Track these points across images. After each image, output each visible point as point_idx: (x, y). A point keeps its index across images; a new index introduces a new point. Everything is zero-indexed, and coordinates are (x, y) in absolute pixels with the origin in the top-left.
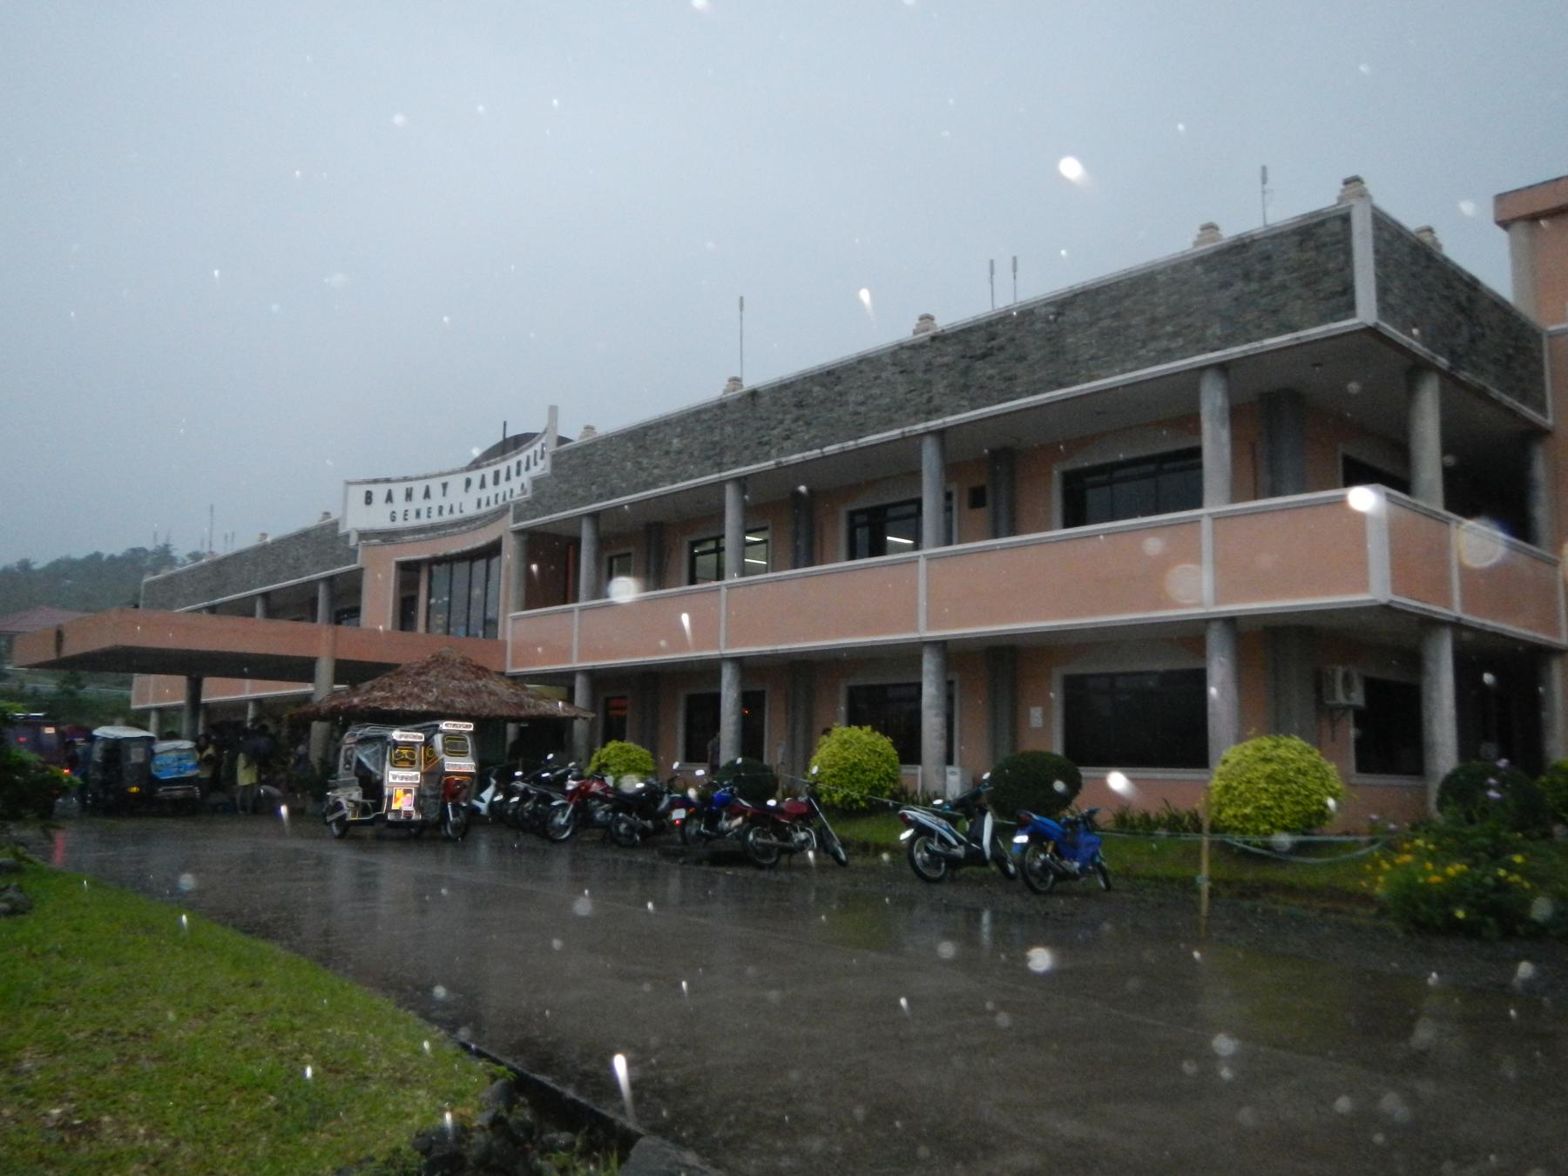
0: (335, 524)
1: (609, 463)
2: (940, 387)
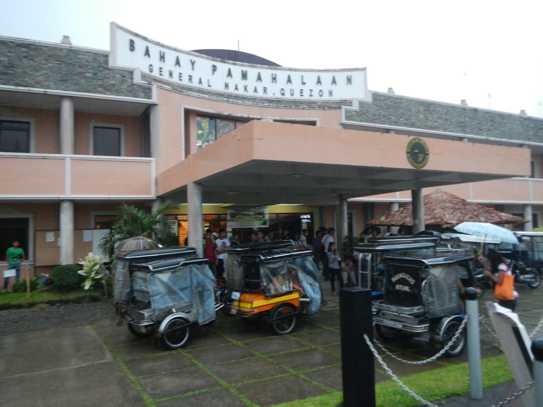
0: (106, 56)
1: (410, 111)
2: (531, 133)
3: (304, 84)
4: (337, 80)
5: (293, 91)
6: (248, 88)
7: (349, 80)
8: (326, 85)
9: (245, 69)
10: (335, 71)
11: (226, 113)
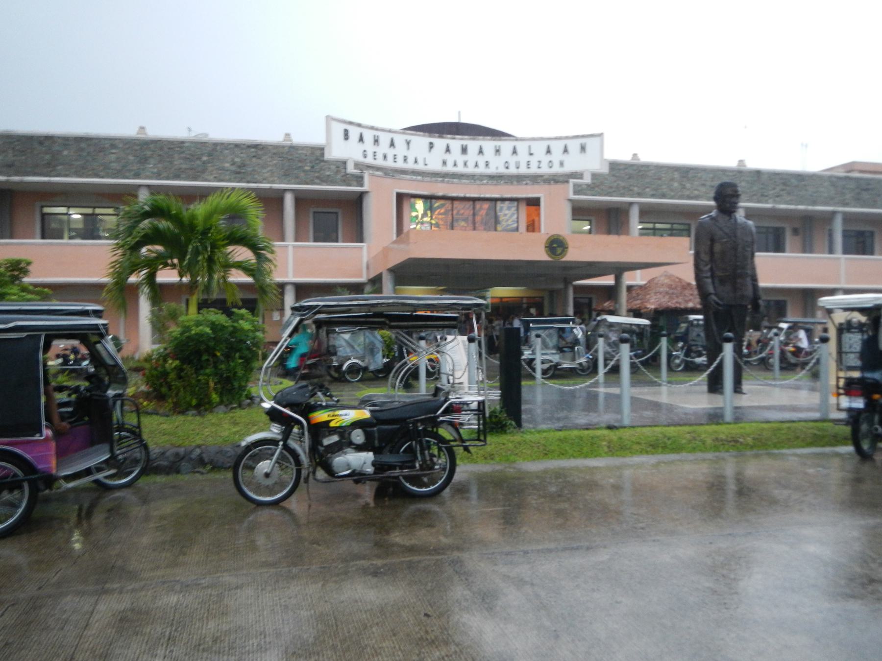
0: (322, 149)
1: (660, 179)
2: (848, 196)
3: (531, 154)
4: (570, 149)
5: (521, 164)
6: (468, 164)
7: (583, 148)
8: (557, 155)
9: (464, 143)
10: (567, 138)
11: (440, 194)
